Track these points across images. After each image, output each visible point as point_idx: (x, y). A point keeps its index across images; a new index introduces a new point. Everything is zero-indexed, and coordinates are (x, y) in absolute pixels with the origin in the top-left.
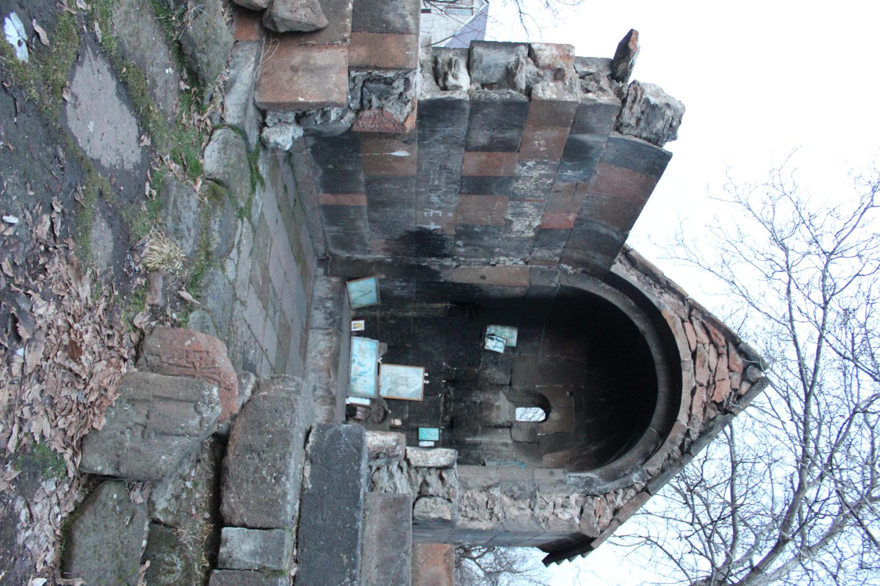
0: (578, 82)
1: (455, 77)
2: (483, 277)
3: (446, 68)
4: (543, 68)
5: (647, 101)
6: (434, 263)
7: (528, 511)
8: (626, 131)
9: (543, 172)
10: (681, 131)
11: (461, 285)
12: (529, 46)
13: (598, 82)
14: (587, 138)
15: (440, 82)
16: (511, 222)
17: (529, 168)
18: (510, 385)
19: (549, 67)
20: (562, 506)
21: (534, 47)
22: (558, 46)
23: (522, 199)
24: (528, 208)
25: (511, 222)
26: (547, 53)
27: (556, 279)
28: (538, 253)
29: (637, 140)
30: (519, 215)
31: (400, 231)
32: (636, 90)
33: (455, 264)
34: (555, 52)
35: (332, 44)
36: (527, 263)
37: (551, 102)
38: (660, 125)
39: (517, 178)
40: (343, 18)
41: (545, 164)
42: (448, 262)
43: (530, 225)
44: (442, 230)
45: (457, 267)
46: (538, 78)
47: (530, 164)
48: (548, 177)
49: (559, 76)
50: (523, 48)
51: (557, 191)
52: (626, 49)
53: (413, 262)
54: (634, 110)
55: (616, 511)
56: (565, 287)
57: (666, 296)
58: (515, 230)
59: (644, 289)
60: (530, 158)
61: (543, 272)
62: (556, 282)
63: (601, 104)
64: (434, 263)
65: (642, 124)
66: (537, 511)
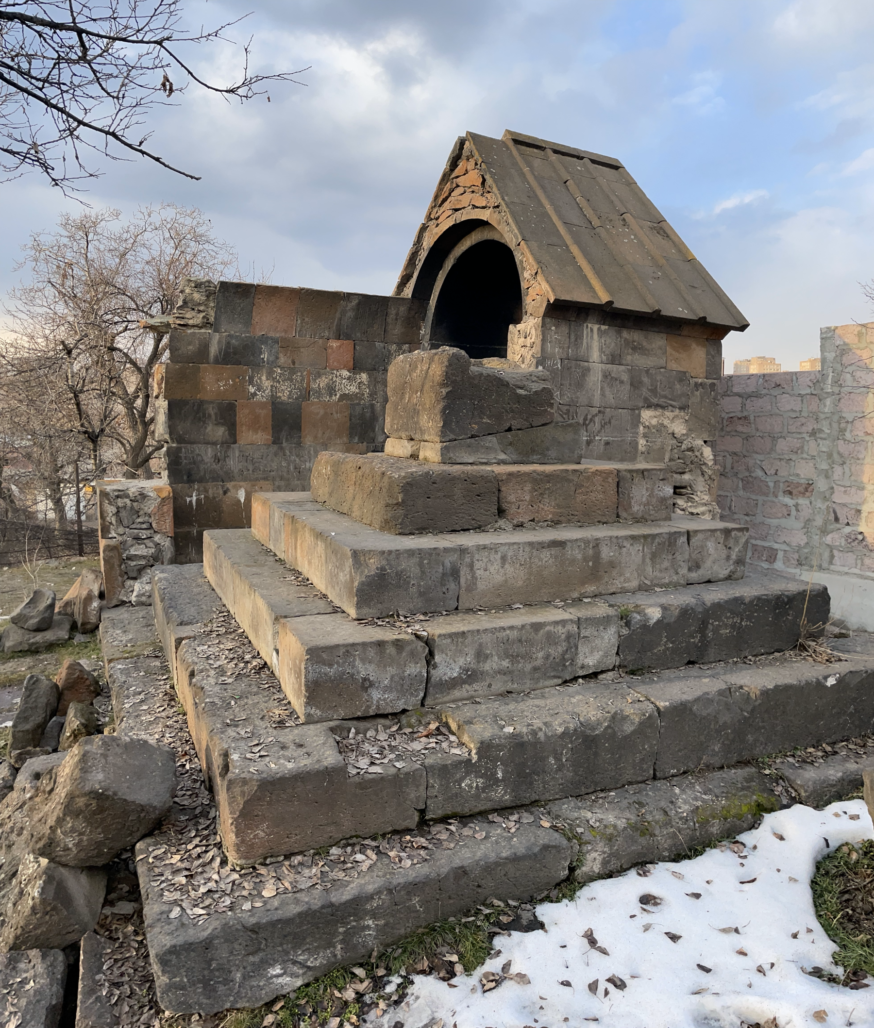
9: (264, 378)
14: (214, 350)
16: (344, 397)
25: (341, 395)
30: (331, 390)
43: (349, 378)
47: (252, 390)
51: (294, 363)
58: (357, 391)
65: (201, 308)
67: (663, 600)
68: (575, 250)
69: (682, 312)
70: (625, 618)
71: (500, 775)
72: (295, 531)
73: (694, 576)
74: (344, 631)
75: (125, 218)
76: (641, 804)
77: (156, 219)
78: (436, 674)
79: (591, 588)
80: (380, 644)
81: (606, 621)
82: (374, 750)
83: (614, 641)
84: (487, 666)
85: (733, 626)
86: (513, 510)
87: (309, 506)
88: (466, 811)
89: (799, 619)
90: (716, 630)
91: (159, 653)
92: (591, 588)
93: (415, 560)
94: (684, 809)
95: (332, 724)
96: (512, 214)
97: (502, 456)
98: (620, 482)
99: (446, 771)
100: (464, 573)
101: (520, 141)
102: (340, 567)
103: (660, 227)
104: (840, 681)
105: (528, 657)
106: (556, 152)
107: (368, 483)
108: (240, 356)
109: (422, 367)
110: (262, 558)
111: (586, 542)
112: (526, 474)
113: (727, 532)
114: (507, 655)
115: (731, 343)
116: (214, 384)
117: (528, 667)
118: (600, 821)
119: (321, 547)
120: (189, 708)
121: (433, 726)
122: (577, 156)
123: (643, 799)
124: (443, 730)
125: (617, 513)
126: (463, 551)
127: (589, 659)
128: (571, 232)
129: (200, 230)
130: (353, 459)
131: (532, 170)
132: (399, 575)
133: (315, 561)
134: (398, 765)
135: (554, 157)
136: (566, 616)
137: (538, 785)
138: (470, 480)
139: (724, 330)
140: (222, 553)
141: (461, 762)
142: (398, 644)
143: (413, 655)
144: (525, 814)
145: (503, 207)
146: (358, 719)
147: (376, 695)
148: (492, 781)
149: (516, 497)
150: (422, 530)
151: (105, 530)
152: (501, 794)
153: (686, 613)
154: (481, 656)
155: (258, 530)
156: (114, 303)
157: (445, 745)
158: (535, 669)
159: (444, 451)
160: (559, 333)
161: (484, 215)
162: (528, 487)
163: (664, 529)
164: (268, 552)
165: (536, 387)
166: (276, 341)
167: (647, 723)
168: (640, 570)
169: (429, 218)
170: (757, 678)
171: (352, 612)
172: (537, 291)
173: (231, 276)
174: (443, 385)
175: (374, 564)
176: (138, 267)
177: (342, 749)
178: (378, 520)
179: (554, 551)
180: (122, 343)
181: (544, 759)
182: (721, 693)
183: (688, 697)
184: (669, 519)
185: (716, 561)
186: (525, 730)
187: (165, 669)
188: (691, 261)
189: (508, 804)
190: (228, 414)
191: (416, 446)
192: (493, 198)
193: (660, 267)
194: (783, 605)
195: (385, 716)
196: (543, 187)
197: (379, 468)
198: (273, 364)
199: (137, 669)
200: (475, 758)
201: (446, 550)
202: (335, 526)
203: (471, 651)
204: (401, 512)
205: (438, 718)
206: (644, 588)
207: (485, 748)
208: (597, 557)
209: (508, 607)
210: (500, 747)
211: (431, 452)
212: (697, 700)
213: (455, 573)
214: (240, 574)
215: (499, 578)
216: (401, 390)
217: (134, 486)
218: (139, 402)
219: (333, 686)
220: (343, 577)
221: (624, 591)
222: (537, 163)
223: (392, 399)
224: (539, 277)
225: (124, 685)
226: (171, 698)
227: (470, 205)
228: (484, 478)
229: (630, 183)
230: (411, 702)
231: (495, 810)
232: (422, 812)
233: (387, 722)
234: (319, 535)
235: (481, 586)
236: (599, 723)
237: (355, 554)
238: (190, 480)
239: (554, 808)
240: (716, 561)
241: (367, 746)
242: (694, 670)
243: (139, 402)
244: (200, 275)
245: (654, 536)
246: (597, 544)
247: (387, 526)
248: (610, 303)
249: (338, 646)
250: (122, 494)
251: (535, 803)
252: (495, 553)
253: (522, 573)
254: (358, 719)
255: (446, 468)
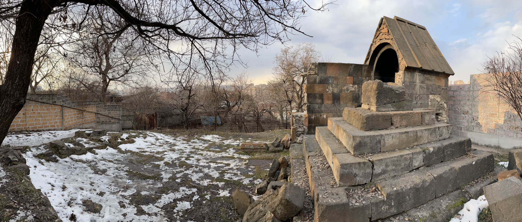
67: (433, 146)
68: (413, 52)
69: (439, 70)
70: (424, 151)
71: (393, 204)
72: (338, 129)
73: (441, 138)
74: (350, 159)
75: (296, 47)
76: (433, 207)
77: (301, 47)
78: (375, 172)
79: (416, 144)
80: (359, 163)
81: (419, 153)
82: (357, 197)
83: (422, 158)
84: (389, 169)
85: (451, 151)
86: (395, 123)
87: (342, 122)
88: (383, 217)
89: (464, 147)
90: (447, 152)
91: (303, 158)
92: (416, 144)
93: (369, 138)
94: (444, 207)
95: (346, 187)
96: (396, 41)
97: (392, 109)
98: (422, 115)
99: (377, 204)
100: (382, 142)
101: (399, 20)
102: (350, 140)
103: (435, 47)
104: (476, 162)
105: (400, 165)
106: (408, 23)
107: (357, 117)
108: (324, 82)
109: (371, 85)
110: (330, 135)
111: (414, 131)
112: (399, 114)
113: (448, 126)
114: (394, 165)
115: (450, 78)
116: (318, 89)
117: (400, 168)
118: (422, 215)
119: (345, 134)
120: (310, 176)
121: (374, 189)
122: (414, 25)
123: (433, 205)
124: (377, 190)
125: (422, 123)
126: (382, 136)
127: (416, 164)
128: (412, 47)
129: (312, 48)
130: (353, 109)
131: (402, 29)
132: (365, 143)
133: (343, 137)
134: (364, 202)
135: (408, 25)
136: (409, 152)
137: (404, 206)
138: (383, 116)
139: (448, 75)
140: (320, 134)
141: (381, 201)
142: (364, 163)
143: (368, 166)
144: (401, 216)
145: (394, 39)
146: (353, 186)
147: (358, 178)
148: (391, 206)
149: (395, 120)
150: (371, 130)
151: (293, 124)
152: (394, 211)
153: (439, 148)
154: (387, 166)
155: (329, 127)
156: (293, 69)
157: (377, 195)
158: (402, 168)
159: (377, 108)
160: (408, 75)
161: (388, 41)
162: (399, 117)
163: (432, 127)
164: (331, 133)
165: (401, 91)
166: (333, 77)
167: (432, 182)
168: (428, 138)
169: (373, 42)
170: (457, 164)
171: (352, 153)
172: (403, 64)
173: (321, 60)
174: (376, 90)
175: (358, 140)
176: (298, 60)
177: (348, 196)
178: (359, 127)
179: (406, 134)
180: (295, 79)
181: (405, 197)
182: (449, 170)
183: (441, 173)
184: (434, 124)
185: (446, 135)
186: (399, 189)
187: (304, 163)
188: (442, 57)
189: (396, 213)
190: (321, 97)
191: (370, 107)
192: (391, 37)
193: (434, 58)
194: (461, 144)
195: (360, 185)
196: (404, 34)
197: (360, 113)
198: (332, 83)
199: (298, 162)
200: (385, 199)
201: (377, 135)
202: (349, 128)
203: (384, 164)
204: (365, 125)
205: (375, 186)
206: (429, 142)
207: (389, 196)
208: (417, 135)
209: (394, 150)
210: (392, 195)
211: (374, 108)
212: (444, 173)
213: (380, 142)
214: (324, 140)
215: (391, 143)
216: (366, 91)
217: (300, 114)
218: (300, 93)
219: (347, 173)
220: (350, 143)
221: (424, 144)
222: (403, 26)
223: (363, 94)
224: (403, 60)
225: (295, 167)
226: (305, 172)
227: (384, 38)
228: (387, 116)
229: (428, 34)
230: (367, 181)
231: (392, 216)
232: (370, 218)
233: (361, 187)
234: (344, 131)
235: (387, 145)
236: (419, 184)
237: (353, 137)
238: (312, 113)
239: (409, 213)
240: (446, 135)
241: (355, 196)
242: (443, 164)
243: (300, 93)
244: (313, 62)
245: (430, 129)
246: (417, 132)
247: (362, 128)
248: (421, 67)
249: (348, 164)
250: (297, 116)
251: (404, 212)
252: (390, 135)
253: (398, 141)
254: (353, 186)
255: (377, 113)
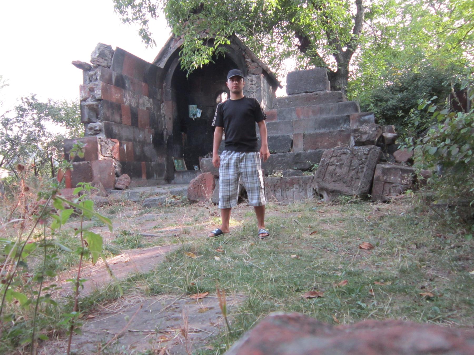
0: (93, 83)
1: (96, 127)
2: (170, 119)
3: (93, 131)
4: (89, 96)
5: (98, 56)
6: (166, 138)
7: (254, 94)
8: (109, 64)
10: (108, 44)
11: (174, 127)
12: (81, 101)
13: (92, 75)
15: (98, 132)
16: (147, 108)
17: (126, 100)
18: (213, 107)
19: (89, 93)
20: (252, 81)
21: (81, 99)
22: (81, 90)
23: (138, 103)
24: (141, 101)
25: (147, 108)
26: (83, 95)
27: (169, 90)
28: (159, 97)
29: (112, 60)
30: (144, 105)
31: (154, 151)
32: (94, 61)
33: (166, 130)
34: (83, 92)
35: (90, 167)
36: (163, 102)
37: (102, 92)
38: (107, 52)
39: (130, 105)
40: (80, 165)
41: (124, 95)
42: (165, 133)
44: (152, 134)
45: (167, 129)
46: (94, 97)
47: (125, 100)
48: (129, 93)
49: (92, 90)
50: (82, 103)
52: (79, 65)
53: (166, 146)
54: (102, 61)
55: (253, 61)
56: (171, 86)
57: (171, 46)
59: (169, 55)
60: (123, 100)
61: (166, 95)
62: (169, 90)
63: (102, 73)
64: (166, 138)
65: (107, 58)
66: (254, 91)
